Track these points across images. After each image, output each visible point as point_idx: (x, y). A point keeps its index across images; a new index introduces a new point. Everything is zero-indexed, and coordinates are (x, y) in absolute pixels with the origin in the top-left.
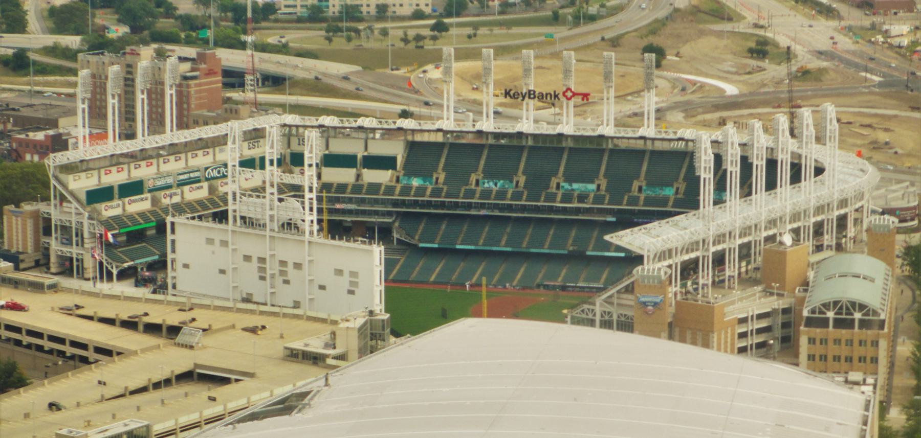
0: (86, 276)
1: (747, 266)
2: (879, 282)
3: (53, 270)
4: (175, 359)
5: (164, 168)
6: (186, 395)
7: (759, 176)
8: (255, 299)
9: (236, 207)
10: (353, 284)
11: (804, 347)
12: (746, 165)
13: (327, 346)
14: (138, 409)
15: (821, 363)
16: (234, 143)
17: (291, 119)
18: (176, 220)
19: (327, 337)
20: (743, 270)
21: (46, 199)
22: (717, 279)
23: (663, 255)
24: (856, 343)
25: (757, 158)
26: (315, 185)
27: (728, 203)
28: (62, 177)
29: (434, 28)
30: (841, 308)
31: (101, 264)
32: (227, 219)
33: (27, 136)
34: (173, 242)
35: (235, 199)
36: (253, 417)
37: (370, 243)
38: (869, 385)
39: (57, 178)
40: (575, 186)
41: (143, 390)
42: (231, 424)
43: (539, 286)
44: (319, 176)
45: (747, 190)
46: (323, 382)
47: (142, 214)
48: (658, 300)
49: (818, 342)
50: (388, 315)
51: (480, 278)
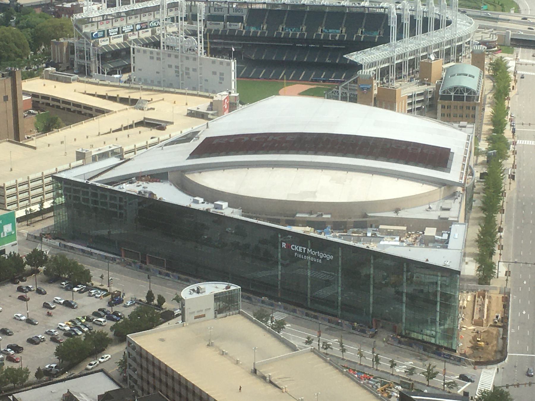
3: (75, 71)
4: (134, 115)
6: (140, 132)
9: (165, 41)
10: (220, 78)
12: (413, 20)
13: (208, 109)
20: (411, 72)
27: (404, 39)
30: (458, 90)
31: (99, 68)
32: (160, 47)
33: (63, 5)
35: (164, 37)
36: (172, 143)
37: (230, 59)
39: (77, 26)
40: (330, 31)
41: (120, 130)
43: (312, 79)
44: (206, 26)
45: (413, 33)
47: (118, 44)
49: (446, 107)
51: (283, 76)
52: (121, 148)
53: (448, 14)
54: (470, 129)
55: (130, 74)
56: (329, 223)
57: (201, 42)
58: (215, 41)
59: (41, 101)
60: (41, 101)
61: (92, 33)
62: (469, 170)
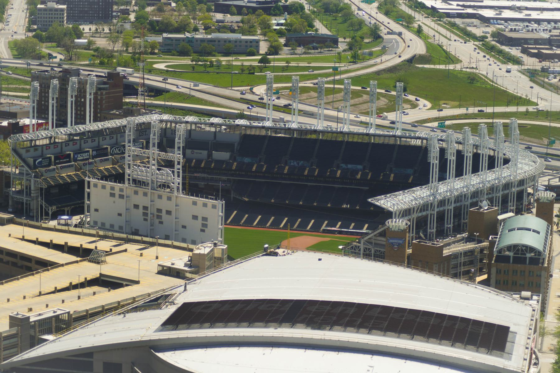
0: (31, 214)
1: (459, 221)
2: (543, 234)
7: (468, 164)
8: (140, 233)
12: (460, 155)
13: (186, 265)
14: (63, 301)
16: (130, 131)
17: (165, 117)
18: (91, 180)
19: (186, 259)
20: (456, 223)
22: (439, 229)
23: (406, 213)
25: (467, 152)
26: (181, 161)
29: (261, 61)
31: (41, 206)
34: (89, 194)
35: (129, 168)
36: (136, 309)
37: (216, 199)
38: (534, 300)
40: (350, 166)
42: (123, 313)
43: (325, 231)
44: (184, 154)
45: (459, 173)
46: (182, 288)
48: (401, 242)
49: (502, 272)
50: (226, 246)
52: (68, 313)
53: (506, 149)
54: (535, 302)
55: (82, 216)
58: (196, 175)
62: (534, 356)
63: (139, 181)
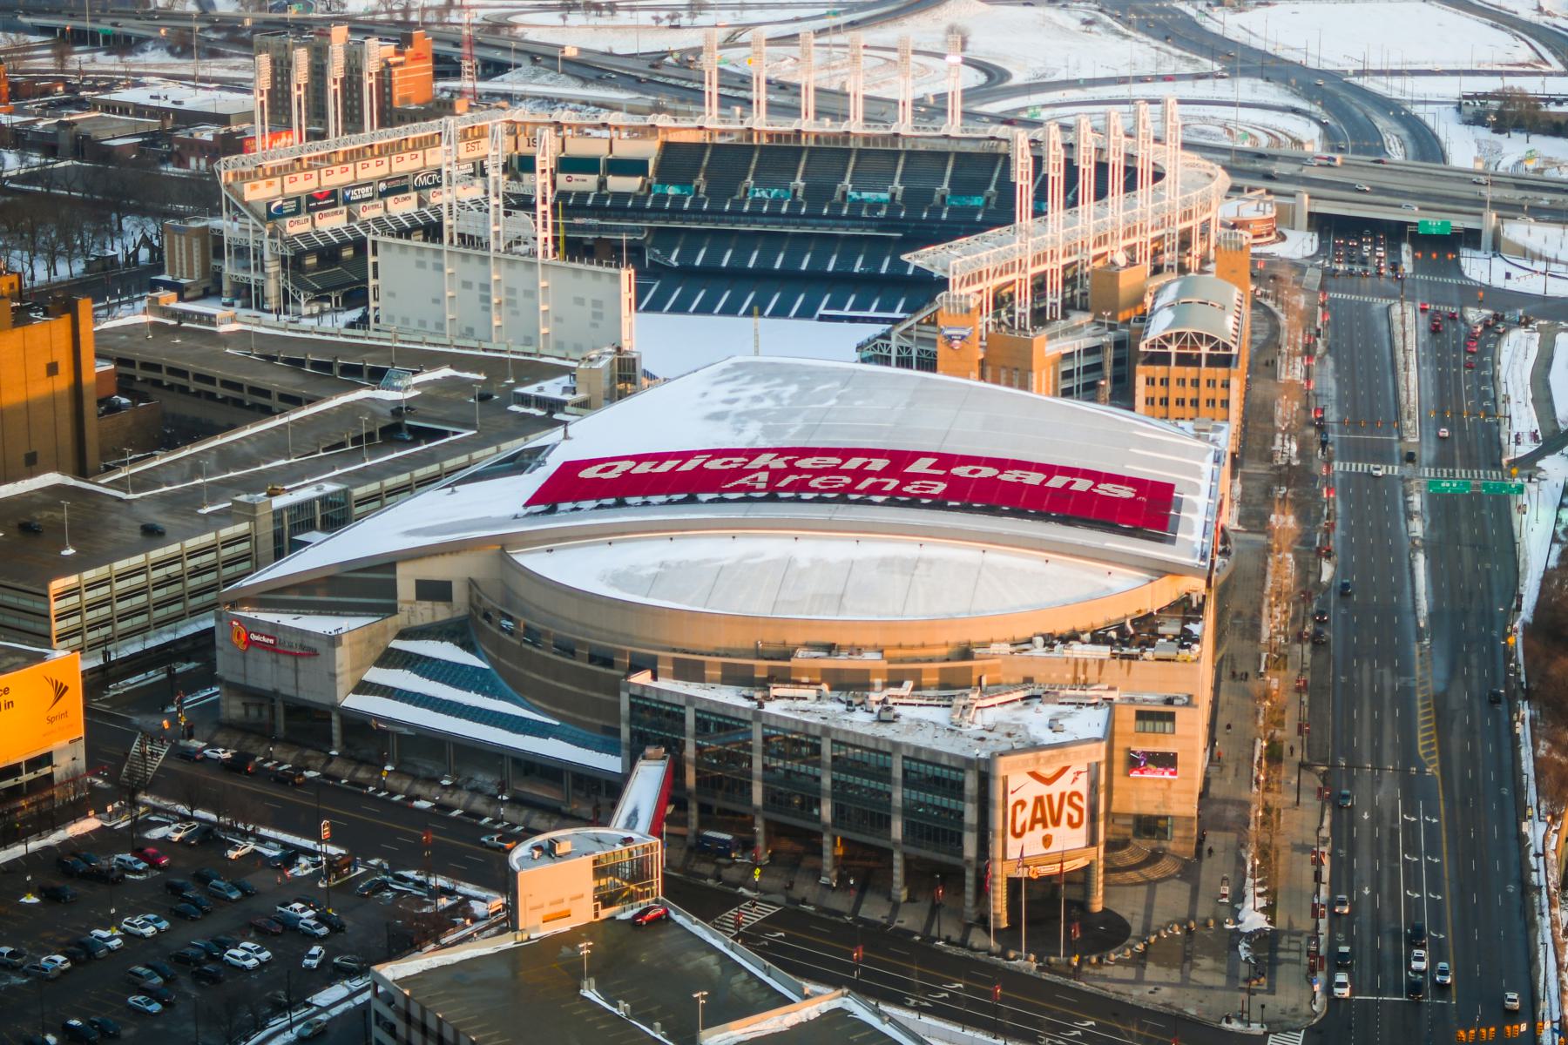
0: (266, 307)
5: (364, 175)
7: (1087, 182)
10: (595, 315)
11: (1141, 390)
12: (1071, 171)
13: (565, 390)
15: (1162, 406)
16: (449, 143)
20: (1068, 295)
21: (216, 212)
24: (1203, 383)
28: (236, 185)
31: (286, 291)
34: (375, 265)
37: (617, 266)
40: (865, 195)
47: (336, 232)
49: (1158, 382)
56: (878, 673)
57: (545, 225)
58: (577, 221)
59: (140, 374)
60: (140, 374)
61: (269, 205)
63: (471, 237)
